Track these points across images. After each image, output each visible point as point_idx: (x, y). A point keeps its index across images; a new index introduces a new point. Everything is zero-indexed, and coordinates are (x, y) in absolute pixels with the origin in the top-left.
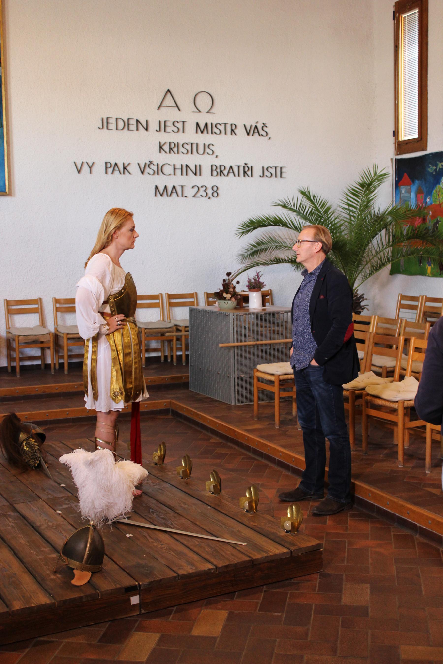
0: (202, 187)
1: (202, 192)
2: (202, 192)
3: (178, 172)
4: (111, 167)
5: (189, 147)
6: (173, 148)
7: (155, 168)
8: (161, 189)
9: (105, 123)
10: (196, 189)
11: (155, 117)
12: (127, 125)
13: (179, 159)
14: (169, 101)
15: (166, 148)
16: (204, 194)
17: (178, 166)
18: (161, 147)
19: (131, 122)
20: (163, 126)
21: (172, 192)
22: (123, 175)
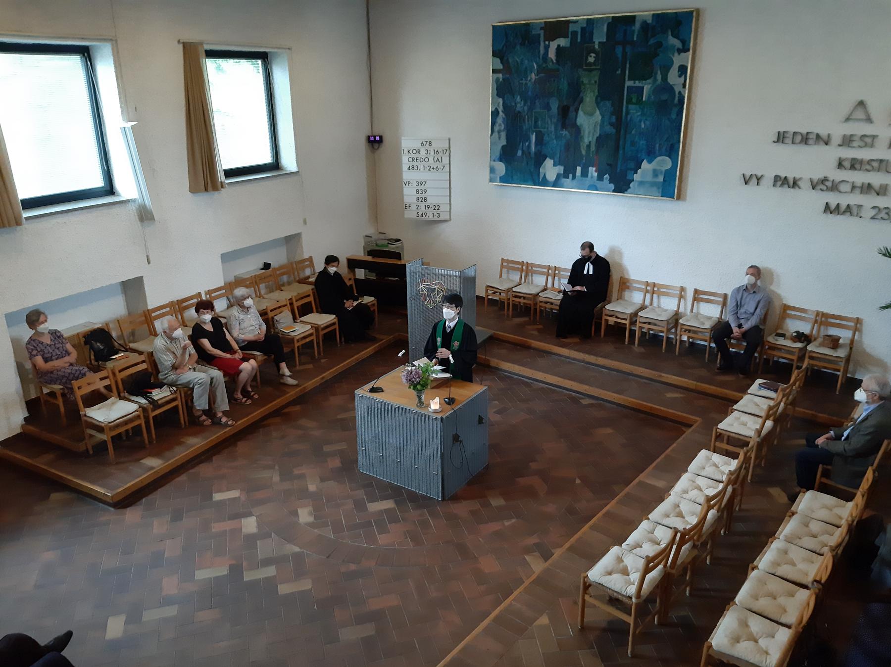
0: (886, 208)
1: (883, 215)
2: (883, 215)
3: (858, 191)
4: (781, 181)
5: (875, 164)
6: (854, 165)
7: (829, 184)
8: (833, 206)
9: (781, 138)
10: (877, 210)
11: (838, 131)
12: (805, 139)
13: (859, 177)
14: (860, 114)
15: (847, 164)
16: (886, 217)
17: (859, 183)
18: (840, 165)
19: (811, 136)
20: (847, 141)
21: (845, 212)
22: (792, 190)
